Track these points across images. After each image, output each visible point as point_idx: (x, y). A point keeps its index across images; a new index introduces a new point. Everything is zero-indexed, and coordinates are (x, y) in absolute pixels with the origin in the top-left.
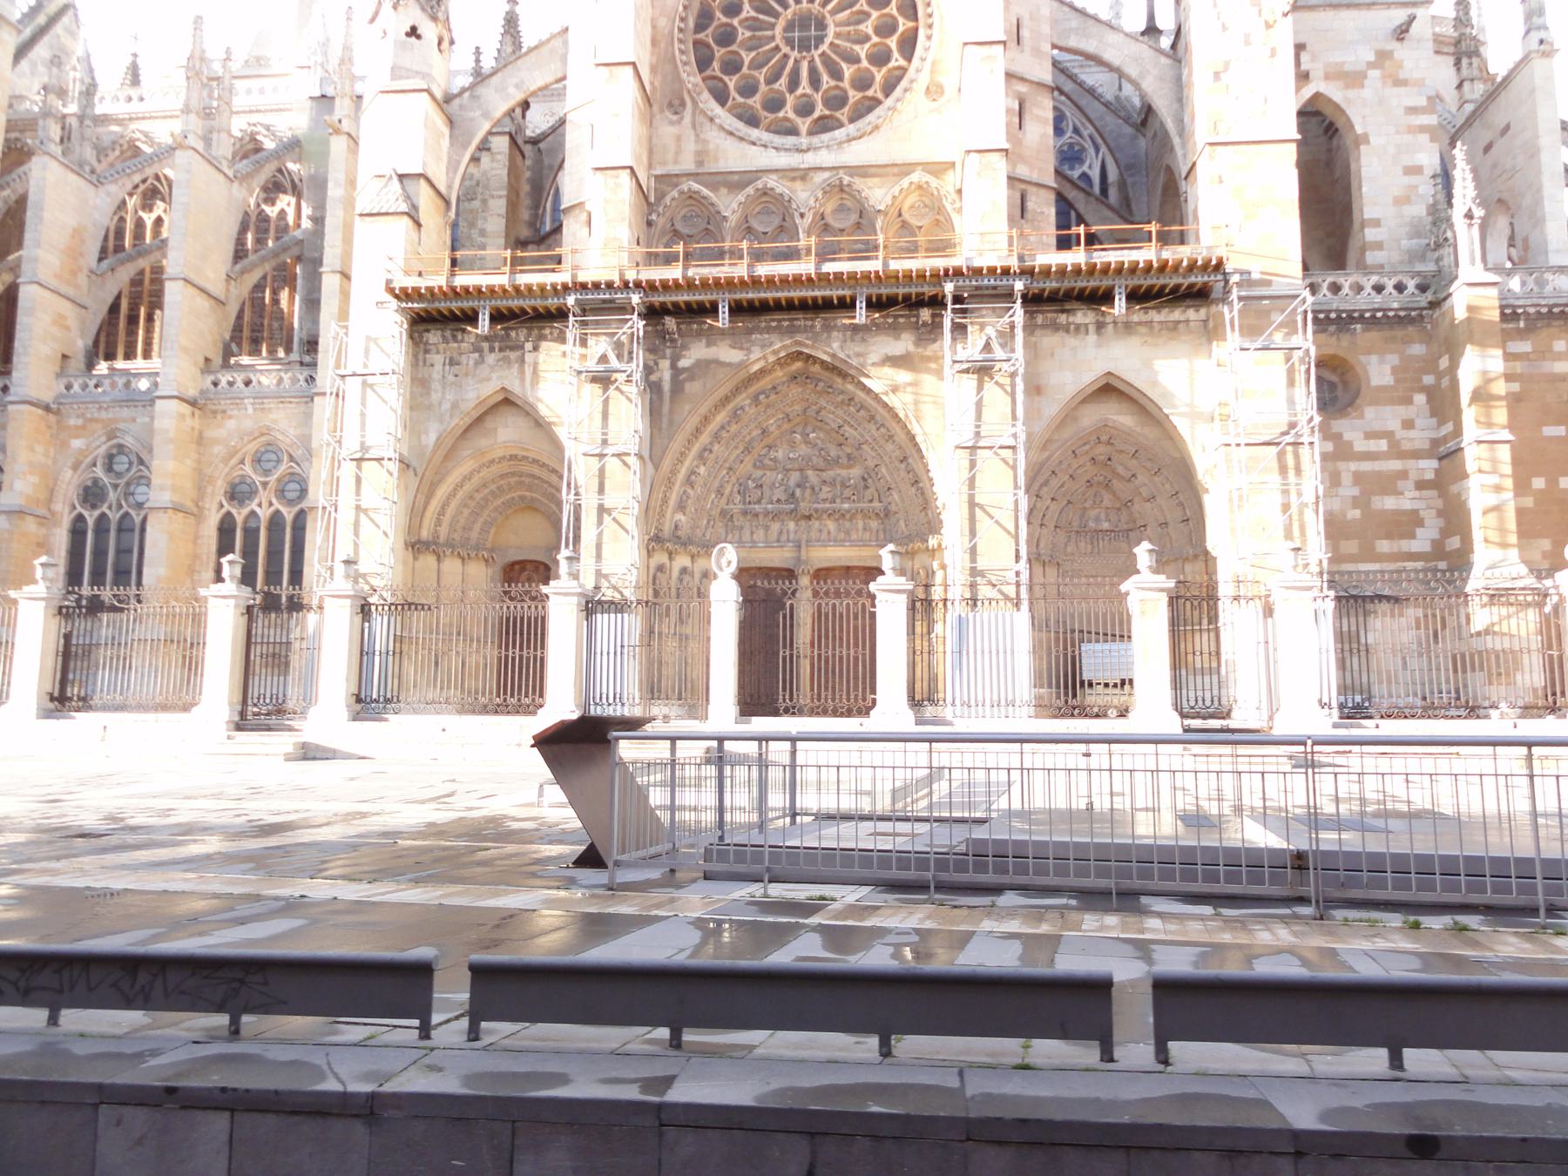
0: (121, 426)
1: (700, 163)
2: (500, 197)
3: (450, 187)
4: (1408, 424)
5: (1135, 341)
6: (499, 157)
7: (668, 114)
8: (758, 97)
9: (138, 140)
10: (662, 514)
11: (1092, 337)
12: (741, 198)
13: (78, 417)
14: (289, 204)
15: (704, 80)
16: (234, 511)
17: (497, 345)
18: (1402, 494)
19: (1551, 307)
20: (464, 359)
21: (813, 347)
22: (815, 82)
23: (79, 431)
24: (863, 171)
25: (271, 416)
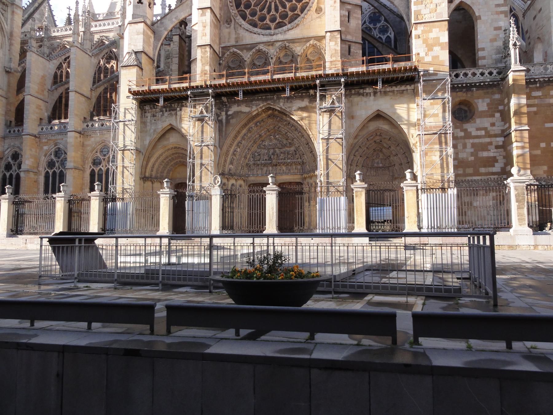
0: (59, 141)
1: (237, 42)
2: (176, 57)
3: (154, 55)
4: (493, 125)
5: (388, 98)
6: (176, 43)
7: (226, 25)
8: (257, 17)
9: (66, 44)
10: (224, 166)
11: (372, 97)
12: (251, 53)
13: (45, 139)
14: (114, 63)
15: (238, 11)
16: (95, 169)
17: (168, 109)
18: (490, 150)
19: (549, 78)
20: (157, 114)
21: (274, 105)
22: (277, 10)
23: (46, 144)
24: (293, 41)
25: (105, 136)
